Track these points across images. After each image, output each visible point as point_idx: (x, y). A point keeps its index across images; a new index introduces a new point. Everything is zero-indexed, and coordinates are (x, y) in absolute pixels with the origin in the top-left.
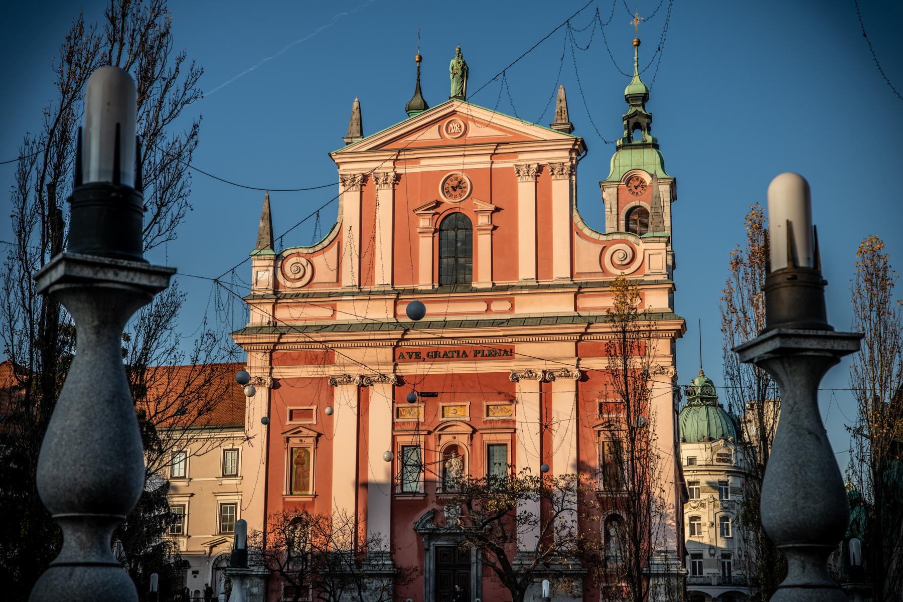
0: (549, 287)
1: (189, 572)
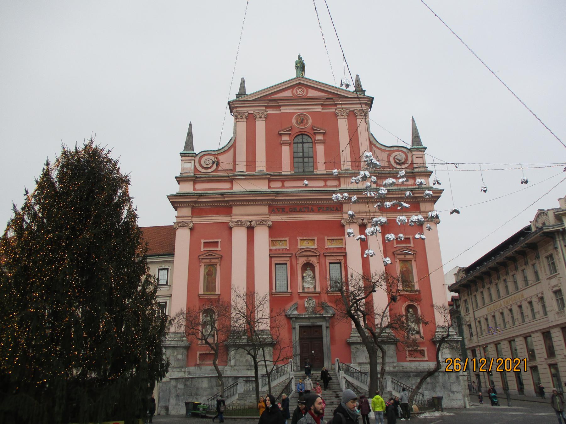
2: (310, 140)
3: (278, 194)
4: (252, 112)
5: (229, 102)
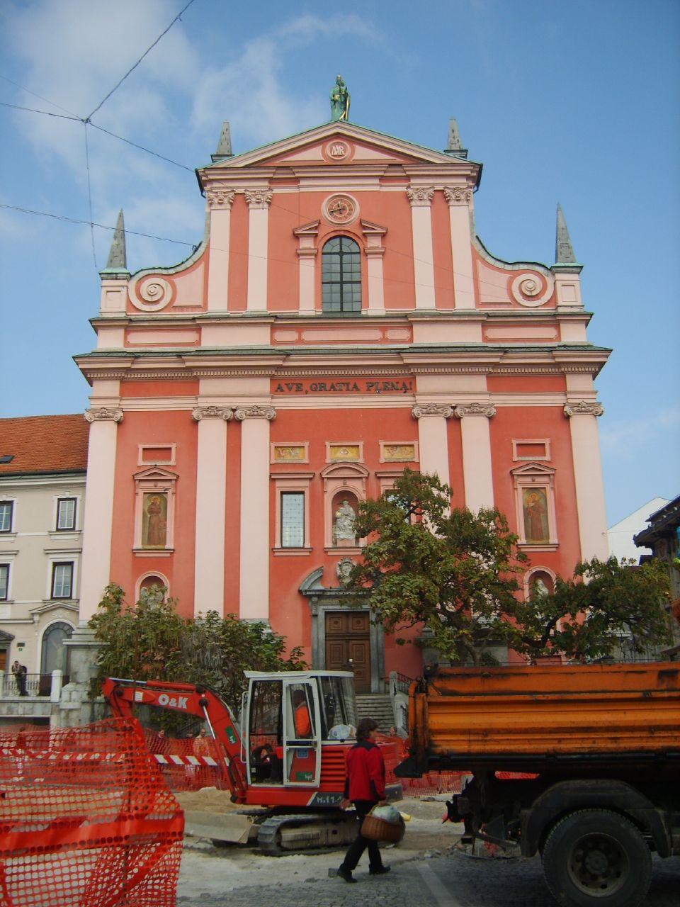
0: (453, 315)
1: (14, 645)
2: (354, 248)
3: (288, 355)
4: (242, 191)
5: (197, 172)
